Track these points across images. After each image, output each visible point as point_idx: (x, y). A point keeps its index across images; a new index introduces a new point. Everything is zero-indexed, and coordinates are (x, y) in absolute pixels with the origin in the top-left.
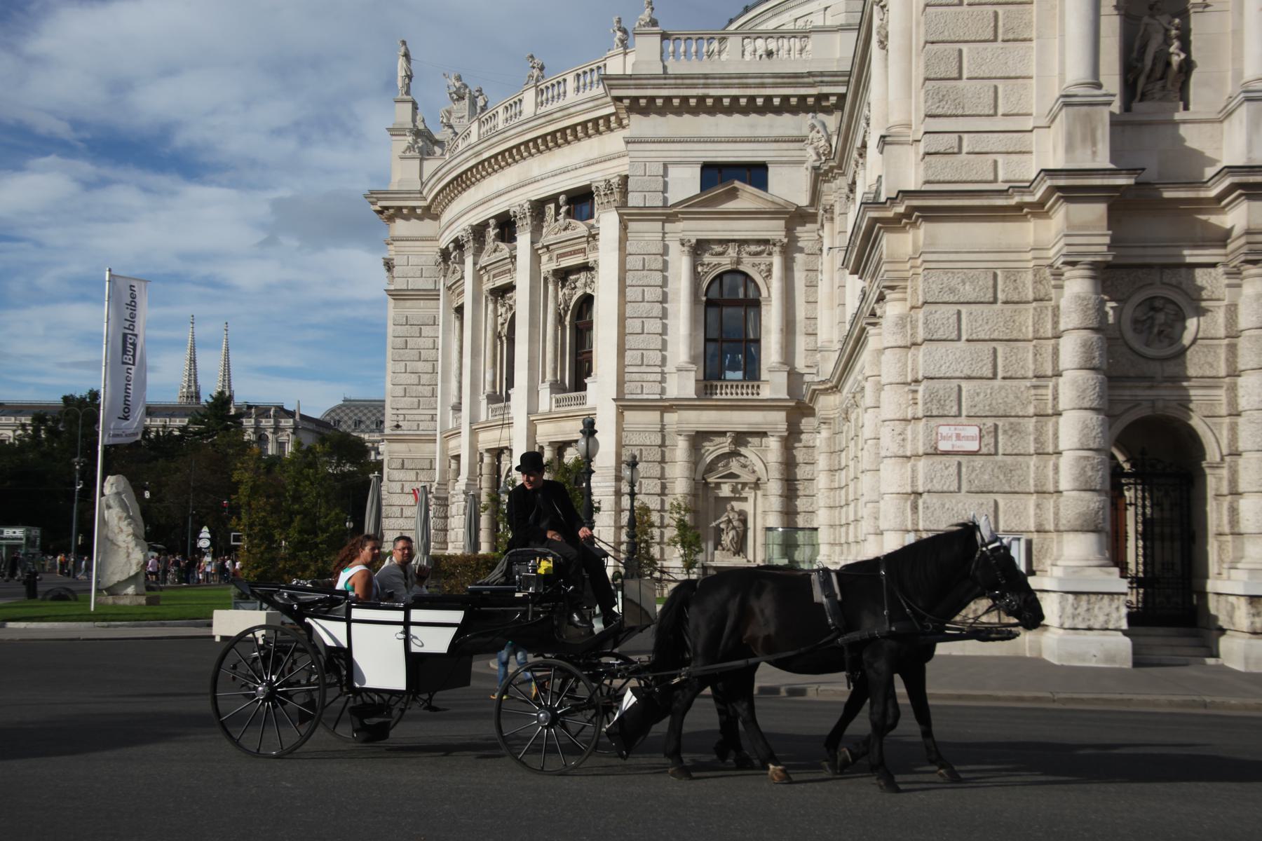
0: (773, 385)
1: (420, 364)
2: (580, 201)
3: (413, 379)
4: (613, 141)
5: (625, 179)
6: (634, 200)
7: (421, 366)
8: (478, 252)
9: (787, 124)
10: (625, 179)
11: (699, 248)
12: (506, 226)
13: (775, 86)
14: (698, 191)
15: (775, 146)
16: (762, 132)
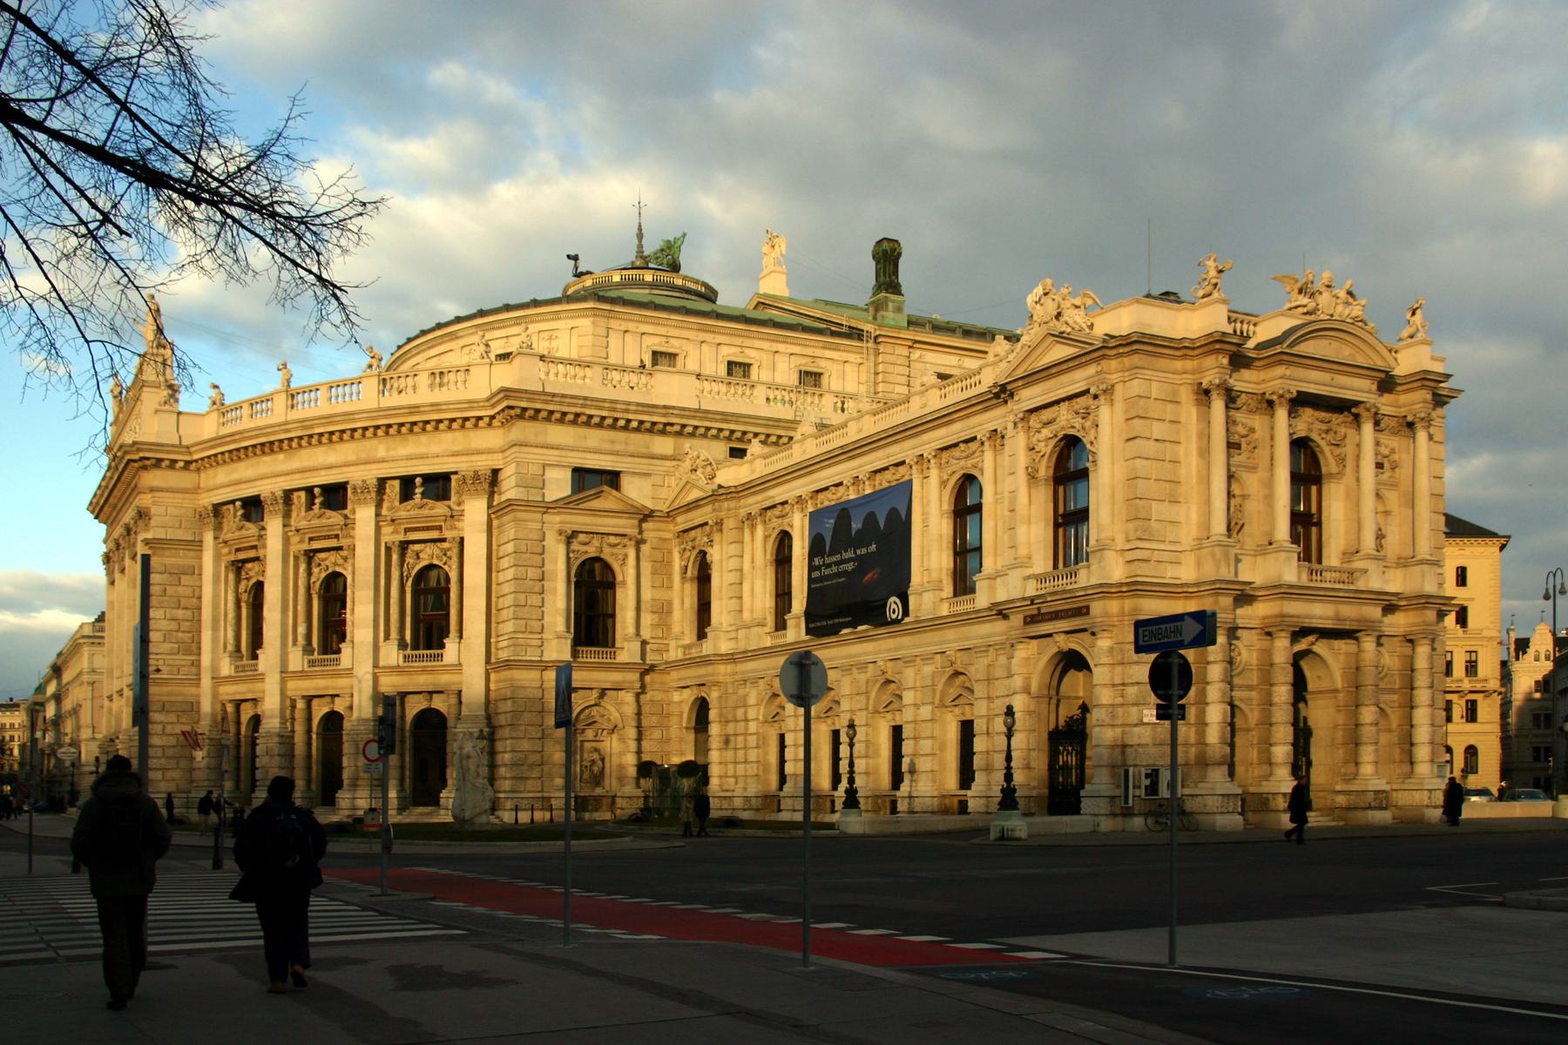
0: (627, 651)
1: (180, 612)
2: (438, 485)
3: (173, 625)
4: (491, 438)
5: (496, 472)
6: (509, 489)
7: (180, 613)
8: (287, 515)
9: (637, 441)
10: (496, 472)
11: (570, 538)
12: (335, 496)
13: (636, 412)
14: (568, 492)
15: (630, 459)
16: (618, 447)
